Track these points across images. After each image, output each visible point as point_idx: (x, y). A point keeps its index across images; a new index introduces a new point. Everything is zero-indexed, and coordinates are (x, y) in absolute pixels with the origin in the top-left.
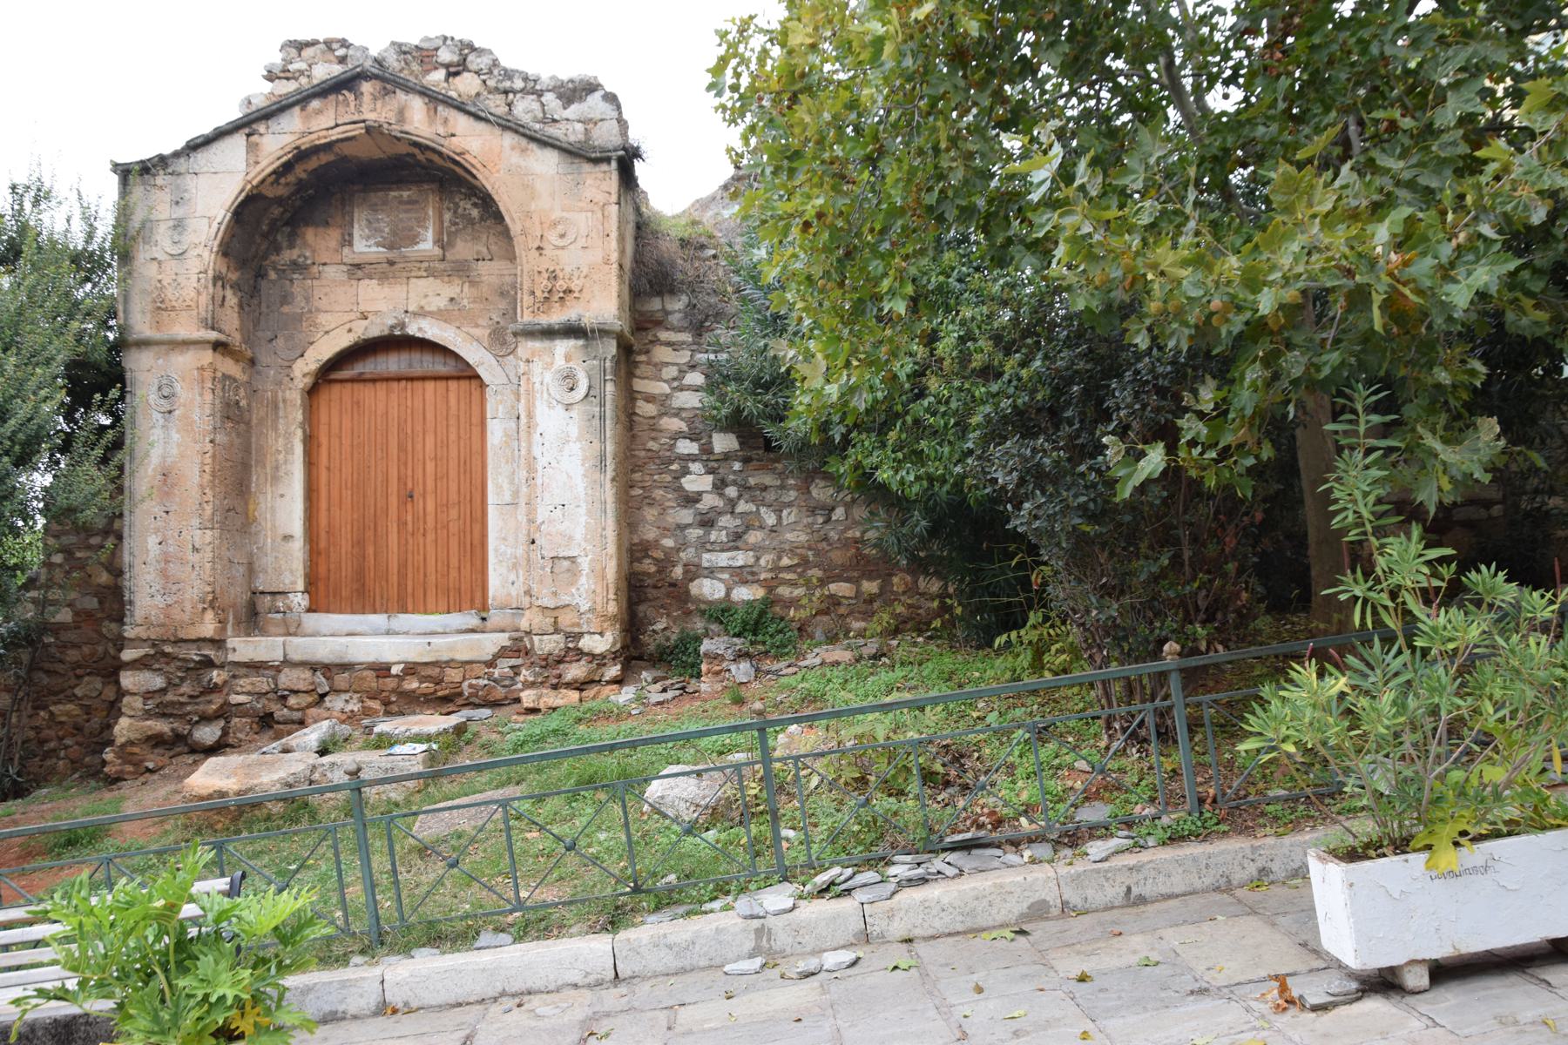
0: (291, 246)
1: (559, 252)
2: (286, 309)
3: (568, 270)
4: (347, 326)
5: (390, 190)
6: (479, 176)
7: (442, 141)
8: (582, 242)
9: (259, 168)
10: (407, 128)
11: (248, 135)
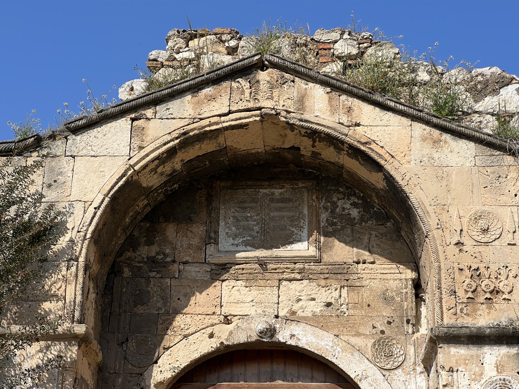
0: (149, 243)
1: (482, 249)
2: (140, 310)
3: (494, 268)
4: (209, 330)
5: (262, 187)
6: (388, 167)
7: (345, 130)
8: (508, 238)
9: (143, 153)
10: (306, 116)
11: (133, 120)
